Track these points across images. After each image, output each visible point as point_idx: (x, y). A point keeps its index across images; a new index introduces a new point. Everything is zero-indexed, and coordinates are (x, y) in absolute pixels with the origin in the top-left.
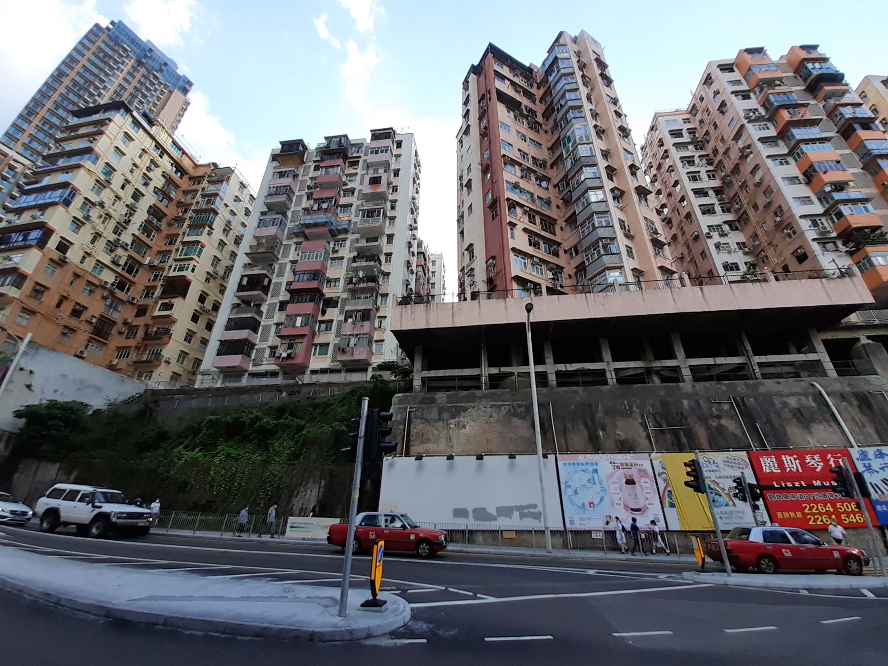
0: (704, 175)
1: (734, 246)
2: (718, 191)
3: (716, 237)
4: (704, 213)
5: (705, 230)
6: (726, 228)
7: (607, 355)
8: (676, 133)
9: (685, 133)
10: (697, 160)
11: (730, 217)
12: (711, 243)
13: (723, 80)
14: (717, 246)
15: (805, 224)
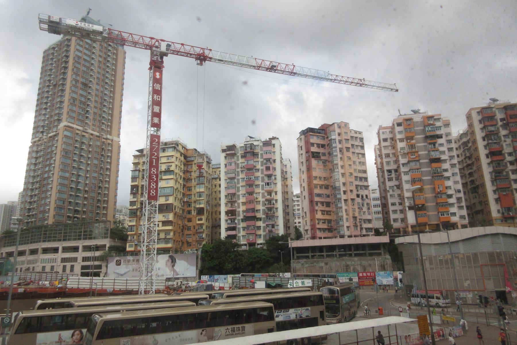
0: (392, 163)
1: (396, 196)
2: (396, 171)
3: (391, 192)
4: (389, 181)
5: (388, 189)
6: (395, 188)
7: (337, 251)
8: (385, 140)
9: (389, 140)
10: (391, 156)
11: (397, 183)
12: (389, 194)
13: (398, 129)
14: (391, 196)
15: (406, 200)
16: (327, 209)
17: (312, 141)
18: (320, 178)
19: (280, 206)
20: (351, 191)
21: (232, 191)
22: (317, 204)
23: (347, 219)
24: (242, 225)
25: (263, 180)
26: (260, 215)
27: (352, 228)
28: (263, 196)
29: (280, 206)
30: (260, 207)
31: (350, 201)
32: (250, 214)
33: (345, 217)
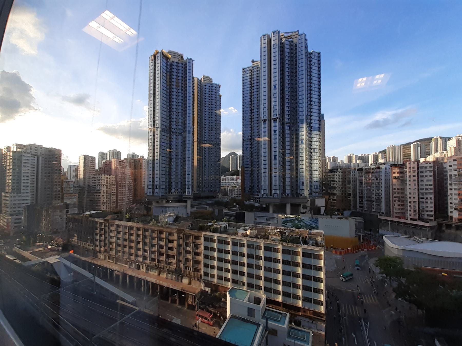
16: (402, 203)
17: (394, 171)
18: (398, 189)
19: (383, 196)
20: (414, 197)
21: (361, 188)
22: (395, 201)
23: (410, 211)
24: (366, 202)
25: (375, 184)
26: (374, 199)
27: (412, 215)
28: (376, 192)
29: (383, 196)
30: (374, 196)
31: (412, 202)
32: (369, 199)
33: (409, 209)
